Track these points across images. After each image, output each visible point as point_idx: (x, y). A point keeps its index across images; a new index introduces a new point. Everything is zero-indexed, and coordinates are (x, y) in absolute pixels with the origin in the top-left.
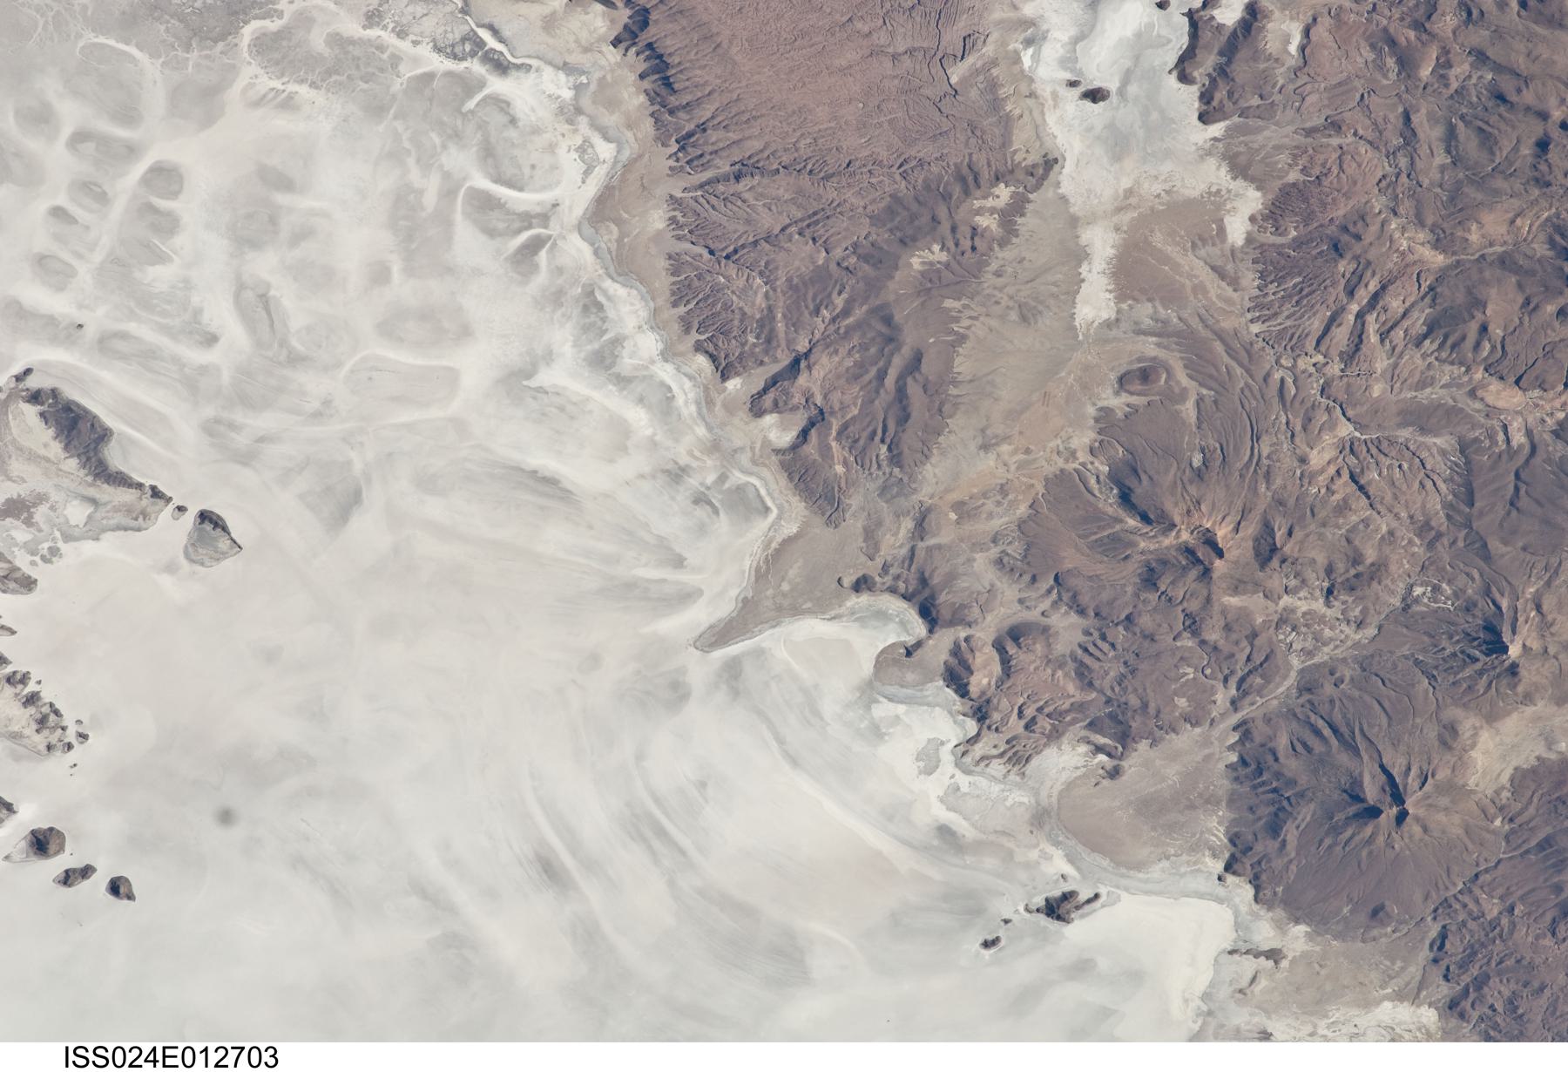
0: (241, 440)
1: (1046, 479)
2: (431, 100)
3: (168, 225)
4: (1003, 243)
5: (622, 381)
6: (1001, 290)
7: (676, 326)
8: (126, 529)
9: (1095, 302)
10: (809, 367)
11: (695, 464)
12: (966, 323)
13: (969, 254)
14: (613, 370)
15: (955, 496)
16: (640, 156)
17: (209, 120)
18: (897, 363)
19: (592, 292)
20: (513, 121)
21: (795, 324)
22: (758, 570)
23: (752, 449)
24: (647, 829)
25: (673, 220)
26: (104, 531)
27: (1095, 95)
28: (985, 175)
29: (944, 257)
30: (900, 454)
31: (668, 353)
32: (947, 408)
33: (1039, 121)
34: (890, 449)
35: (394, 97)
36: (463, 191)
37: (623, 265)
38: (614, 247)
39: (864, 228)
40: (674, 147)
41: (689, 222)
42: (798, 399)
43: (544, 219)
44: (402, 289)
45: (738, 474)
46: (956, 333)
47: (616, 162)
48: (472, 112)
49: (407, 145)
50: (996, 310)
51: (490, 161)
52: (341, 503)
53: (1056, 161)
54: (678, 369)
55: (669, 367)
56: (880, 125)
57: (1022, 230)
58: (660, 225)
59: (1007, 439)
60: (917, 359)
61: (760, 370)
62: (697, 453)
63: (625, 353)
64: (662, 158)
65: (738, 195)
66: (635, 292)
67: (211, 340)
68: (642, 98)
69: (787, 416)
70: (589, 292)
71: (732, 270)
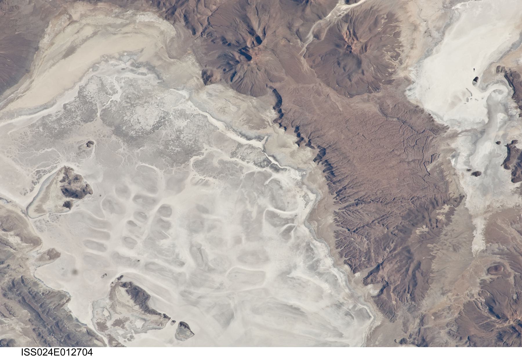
0: (193, 298)
1: (464, 304)
2: (254, 181)
3: (167, 226)
4: (447, 224)
5: (320, 274)
6: (447, 240)
7: (338, 255)
9: (478, 244)
10: (383, 268)
11: (345, 302)
12: (435, 252)
13: (435, 228)
15: (433, 311)
16: (324, 198)
17: (180, 190)
18: (412, 266)
19: (309, 245)
20: (281, 188)
21: (377, 254)
23: (364, 296)
25: (335, 219)
27: (476, 174)
28: (440, 202)
29: (427, 230)
30: (414, 297)
31: (335, 265)
32: (430, 281)
33: (458, 183)
34: (411, 295)
35: (241, 180)
36: (265, 212)
37: (319, 235)
38: (316, 229)
39: (400, 220)
40: (335, 195)
41: (341, 220)
42: (379, 279)
43: (292, 220)
44: (247, 245)
45: (360, 305)
46: (432, 255)
47: (316, 200)
49: (246, 197)
50: (445, 247)
51: (274, 201)
52: (227, 318)
53: (464, 196)
54: (339, 270)
55: (336, 269)
56: (404, 185)
57: (453, 220)
58: (331, 221)
59: (450, 291)
60: (419, 264)
61: (366, 269)
62: (346, 298)
63: (321, 265)
64: (331, 199)
65: (357, 211)
66: (323, 244)
67: (182, 264)
68: (324, 179)
69: (376, 285)
70: (308, 245)
71: (356, 236)
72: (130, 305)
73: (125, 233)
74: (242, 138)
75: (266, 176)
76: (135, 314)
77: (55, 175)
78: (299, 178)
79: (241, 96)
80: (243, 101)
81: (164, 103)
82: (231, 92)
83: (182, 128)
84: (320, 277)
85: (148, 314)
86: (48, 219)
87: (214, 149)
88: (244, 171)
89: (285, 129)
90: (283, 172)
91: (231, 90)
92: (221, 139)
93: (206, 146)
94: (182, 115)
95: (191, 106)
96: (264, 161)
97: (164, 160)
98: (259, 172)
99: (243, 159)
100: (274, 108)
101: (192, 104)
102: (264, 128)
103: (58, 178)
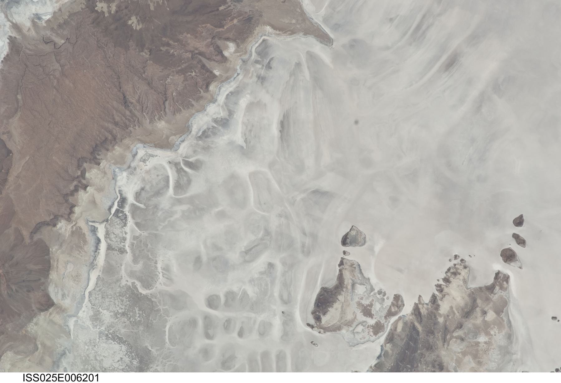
0: (308, 241)
3: (230, 296)
5: (231, 113)
7: (201, 102)
8: (361, 270)
11: (255, 74)
14: (227, 117)
19: (199, 137)
20: (143, 189)
22: (291, 34)
23: (240, 56)
24: (418, 34)
26: (364, 277)
31: (213, 100)
35: (149, 234)
37: (185, 129)
38: (178, 136)
43: (176, 164)
48: (145, 205)
51: (161, 192)
62: (250, 75)
63: (219, 116)
65: (138, 101)
67: (271, 265)
68: (116, 147)
70: (200, 138)
72: (340, 306)
73: (255, 336)
74: (101, 248)
75: (135, 209)
76: (349, 298)
78: (125, 174)
79: (54, 263)
80: (58, 260)
81: (90, 340)
82: (53, 275)
83: (112, 314)
84: (234, 111)
85: (345, 283)
87: (123, 273)
88: (137, 234)
89: (73, 206)
90: (123, 193)
91: (51, 277)
92: (110, 270)
93: (123, 283)
94: (96, 318)
95: (84, 312)
96: (118, 217)
97: (154, 321)
98: (133, 217)
99: (124, 239)
100: (55, 225)
101: (81, 312)
102: (80, 229)
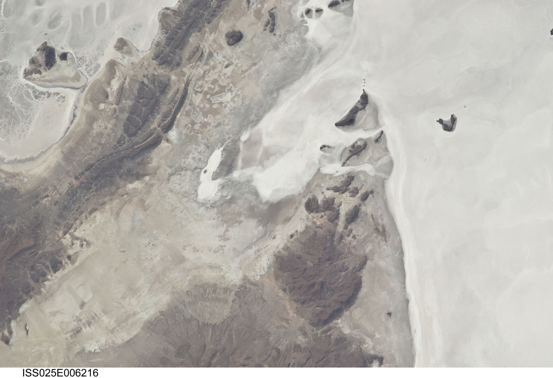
77: (35, 81)
86: (84, 67)
103: (38, 78)
